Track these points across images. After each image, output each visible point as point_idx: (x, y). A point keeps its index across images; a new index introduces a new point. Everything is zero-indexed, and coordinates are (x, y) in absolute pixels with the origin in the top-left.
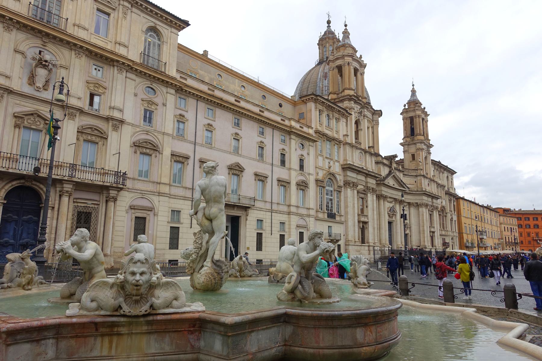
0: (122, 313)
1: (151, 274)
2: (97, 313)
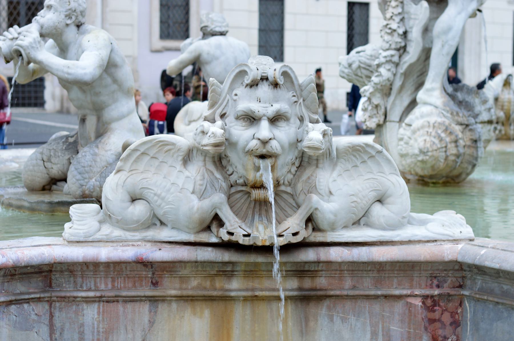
0: (226, 237)
1: (301, 119)
2: (151, 234)
